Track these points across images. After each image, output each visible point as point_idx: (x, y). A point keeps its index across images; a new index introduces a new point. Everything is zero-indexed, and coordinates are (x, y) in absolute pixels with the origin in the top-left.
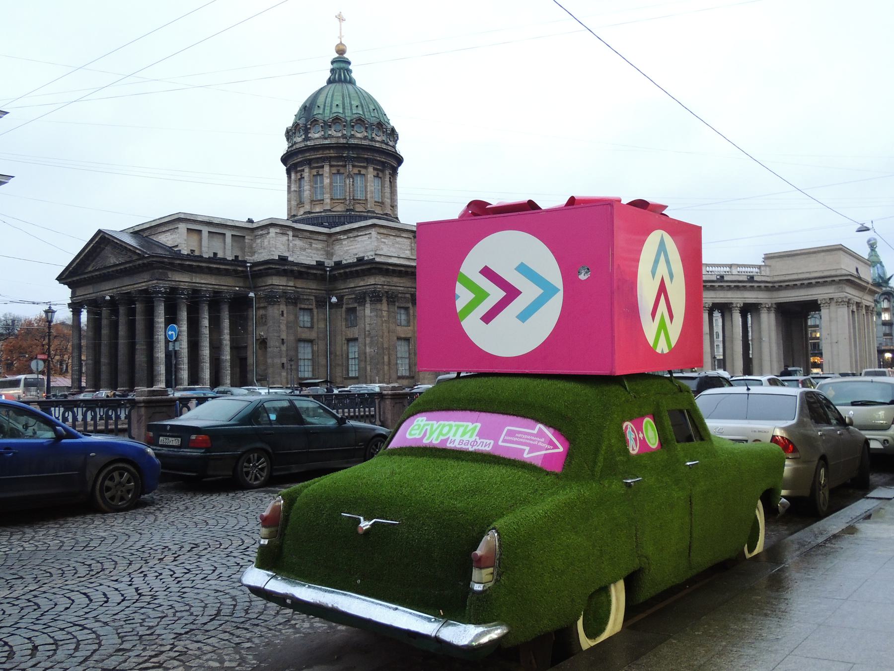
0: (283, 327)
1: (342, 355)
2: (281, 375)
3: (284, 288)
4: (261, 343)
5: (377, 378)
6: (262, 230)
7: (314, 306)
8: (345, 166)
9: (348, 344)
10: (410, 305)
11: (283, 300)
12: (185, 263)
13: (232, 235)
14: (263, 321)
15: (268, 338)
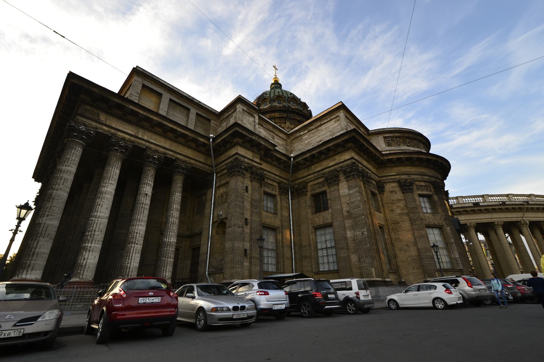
0: (247, 205)
1: (310, 245)
2: (243, 265)
3: (250, 162)
4: (218, 226)
5: (373, 269)
6: (227, 113)
7: (276, 193)
8: (285, 123)
9: (315, 233)
10: (377, 192)
11: (248, 175)
12: (127, 106)
13: (197, 113)
14: (222, 200)
15: (229, 216)
